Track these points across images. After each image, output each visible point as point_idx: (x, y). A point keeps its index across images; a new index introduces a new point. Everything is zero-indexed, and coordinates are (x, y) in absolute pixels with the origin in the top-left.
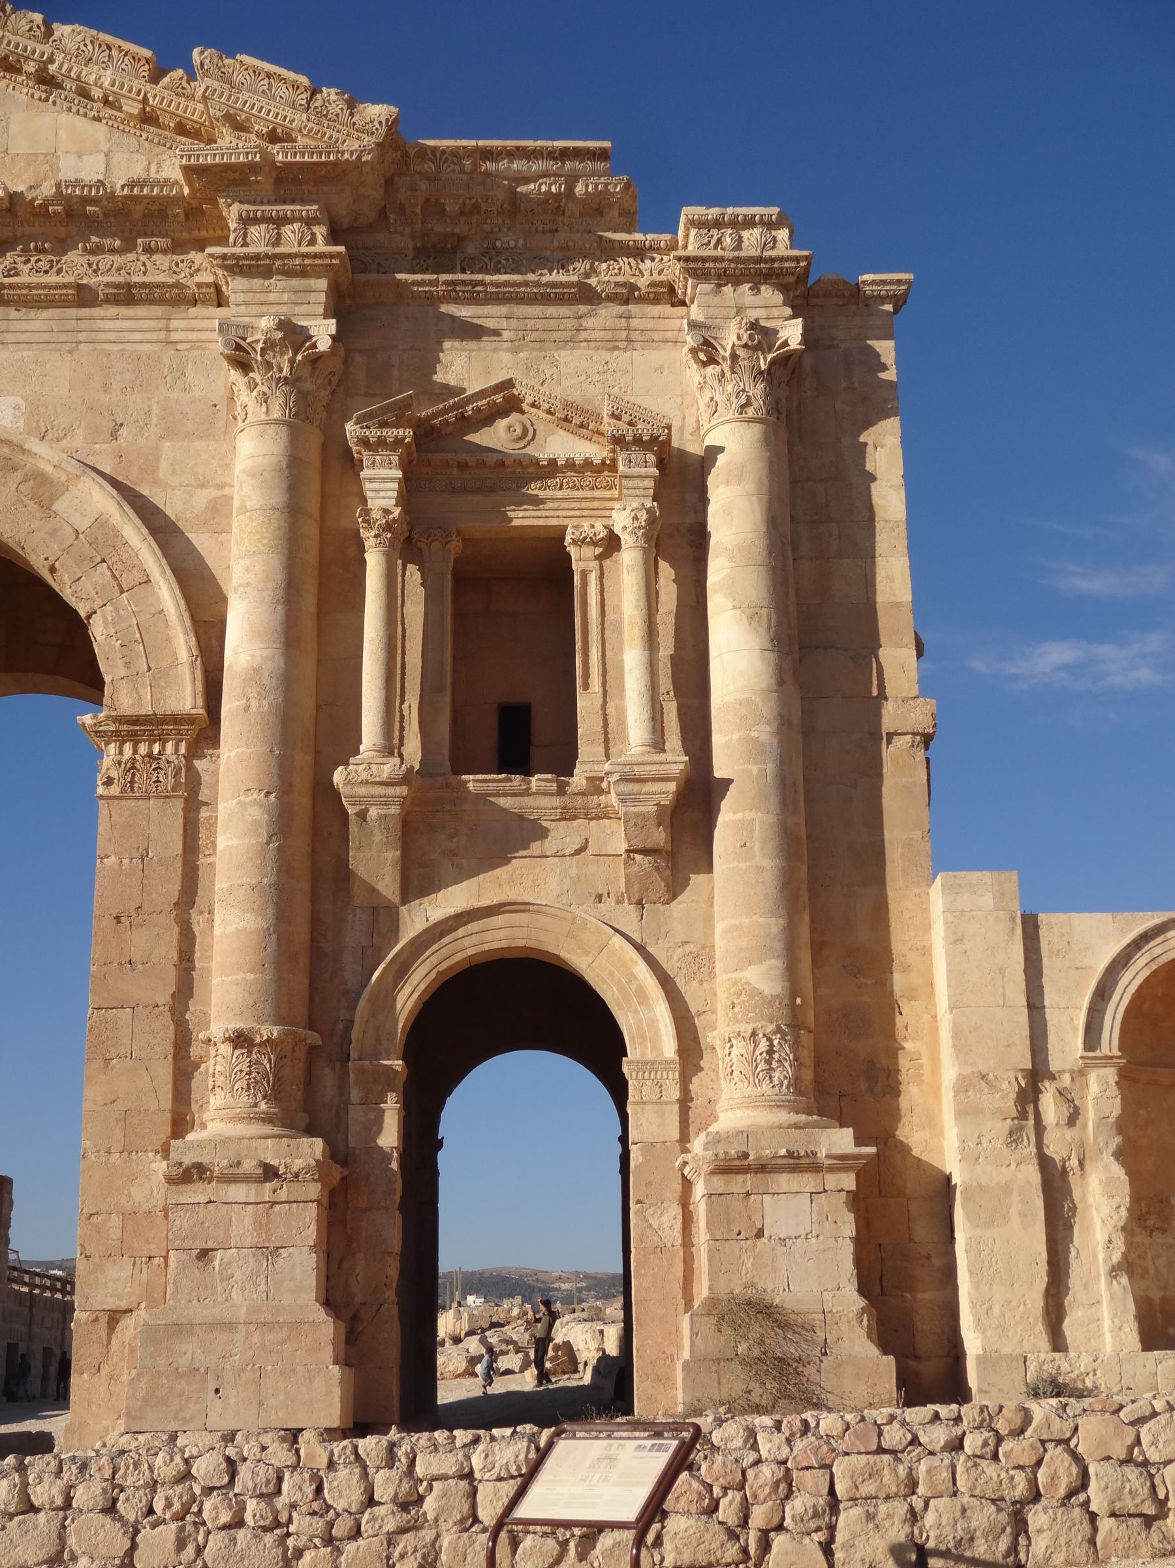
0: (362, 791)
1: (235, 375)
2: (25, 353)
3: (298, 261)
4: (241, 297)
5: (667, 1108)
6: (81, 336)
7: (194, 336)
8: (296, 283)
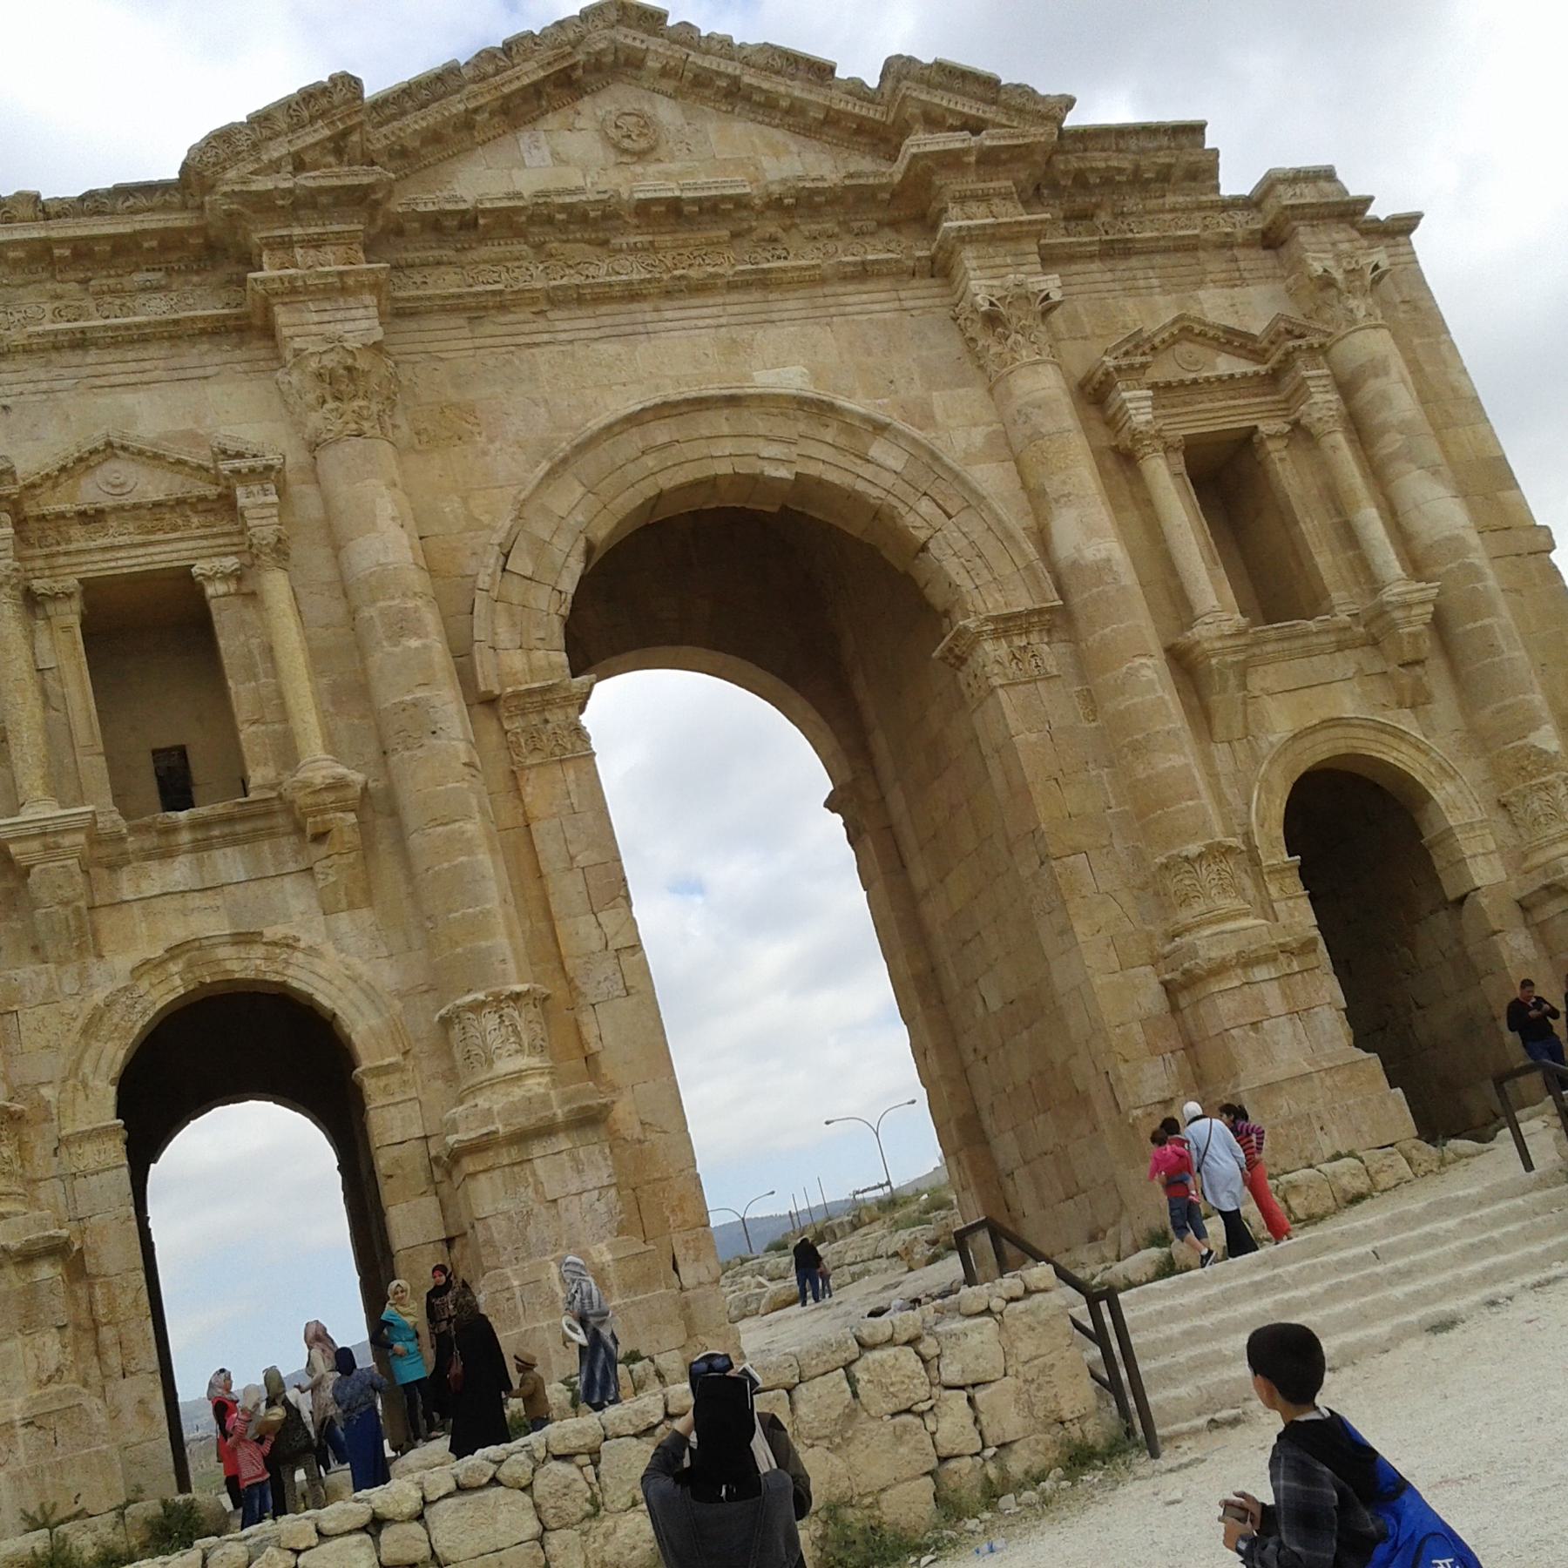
0: (1218, 645)
1: (975, 330)
2: (792, 329)
3: (1016, 229)
4: (974, 263)
5: (1491, 856)
6: (833, 310)
7: (920, 303)
8: (1010, 246)
